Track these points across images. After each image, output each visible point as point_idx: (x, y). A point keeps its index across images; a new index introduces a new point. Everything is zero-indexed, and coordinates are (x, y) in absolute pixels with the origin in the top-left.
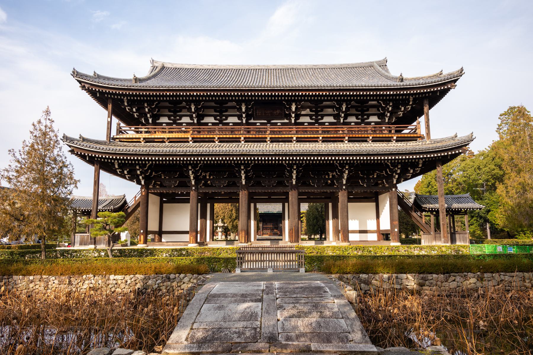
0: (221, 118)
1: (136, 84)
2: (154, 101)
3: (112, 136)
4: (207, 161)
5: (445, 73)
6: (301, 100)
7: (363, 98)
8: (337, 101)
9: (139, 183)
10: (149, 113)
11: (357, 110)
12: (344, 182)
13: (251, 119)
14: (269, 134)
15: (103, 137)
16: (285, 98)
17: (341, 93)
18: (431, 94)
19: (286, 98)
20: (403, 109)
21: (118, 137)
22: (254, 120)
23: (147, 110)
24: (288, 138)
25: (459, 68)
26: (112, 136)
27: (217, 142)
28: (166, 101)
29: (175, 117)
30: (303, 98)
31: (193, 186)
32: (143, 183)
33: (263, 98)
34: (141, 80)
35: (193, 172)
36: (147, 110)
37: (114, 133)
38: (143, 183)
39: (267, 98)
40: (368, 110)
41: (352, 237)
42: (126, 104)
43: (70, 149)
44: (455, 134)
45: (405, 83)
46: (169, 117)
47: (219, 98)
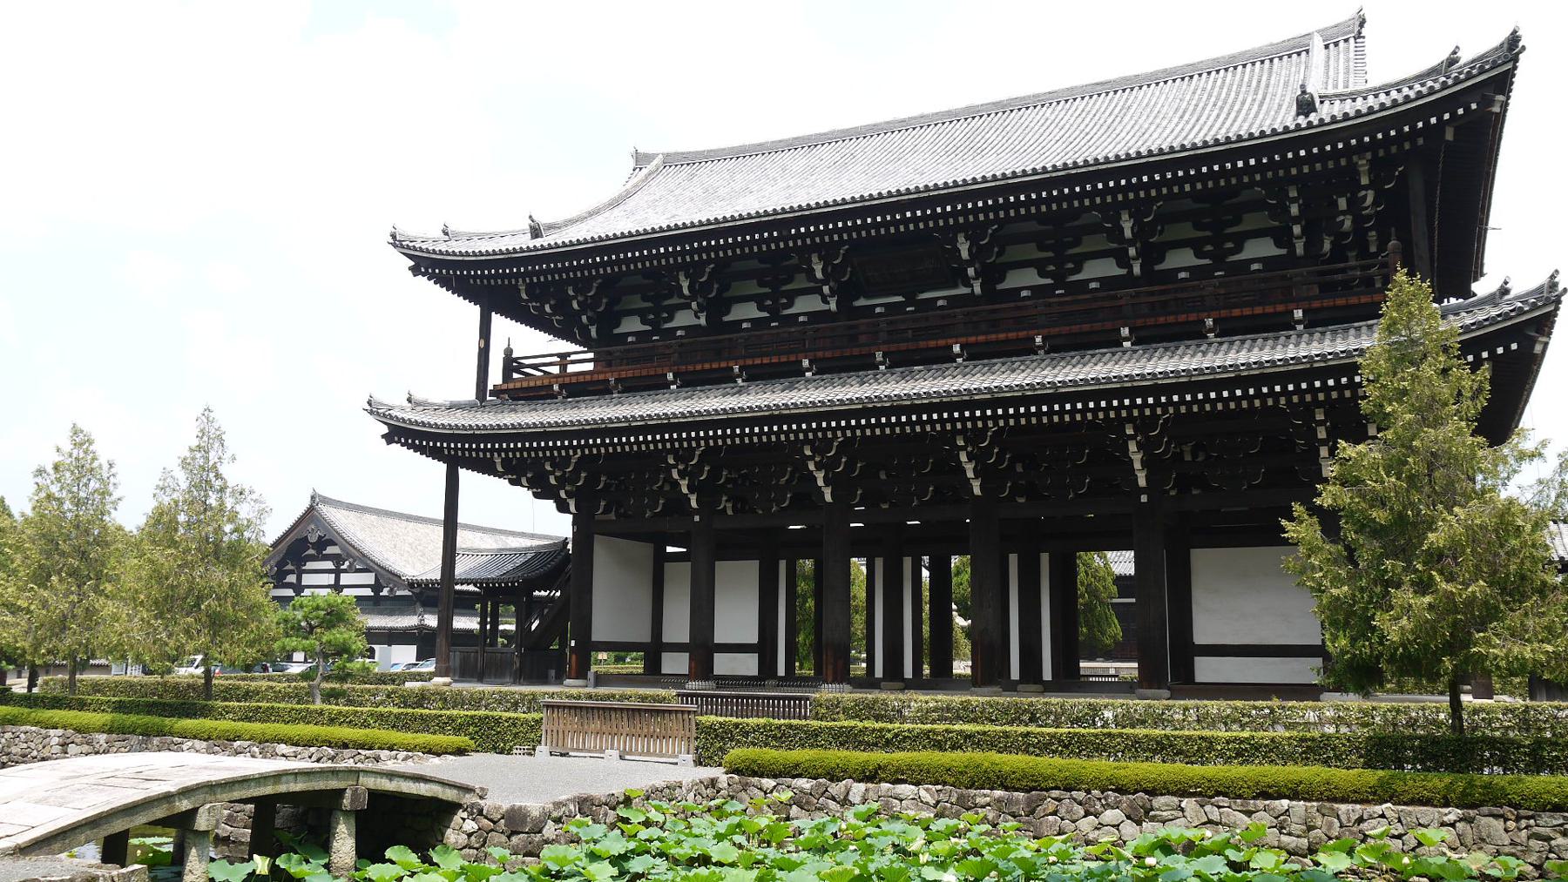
0: (775, 301)
1: (538, 242)
2: (591, 278)
3: (490, 387)
4: (786, 434)
5: (1466, 56)
6: (988, 223)
7: (1300, 170)
8: (1103, 207)
9: (562, 507)
10: (583, 310)
11: (1197, 226)
12: (1142, 482)
13: (857, 298)
14: (884, 343)
15: (470, 394)
16: (936, 223)
17: (1134, 180)
18: (1421, 141)
19: (941, 223)
20: (1342, 203)
21: (511, 386)
22: (868, 297)
23: (575, 306)
24: (938, 348)
25: (1501, 36)
26: (490, 387)
27: (739, 381)
28: (752, 255)
29: (657, 314)
30: (1087, 202)
31: (696, 512)
32: (572, 508)
33: (902, 228)
34: (551, 227)
35: (682, 474)
36: (575, 306)
37: (495, 377)
38: (572, 508)
39: (921, 226)
40: (1238, 221)
41: (1207, 670)
42: (524, 296)
43: (385, 430)
44: (1501, 283)
45: (1325, 111)
46: (642, 314)
47: (769, 247)
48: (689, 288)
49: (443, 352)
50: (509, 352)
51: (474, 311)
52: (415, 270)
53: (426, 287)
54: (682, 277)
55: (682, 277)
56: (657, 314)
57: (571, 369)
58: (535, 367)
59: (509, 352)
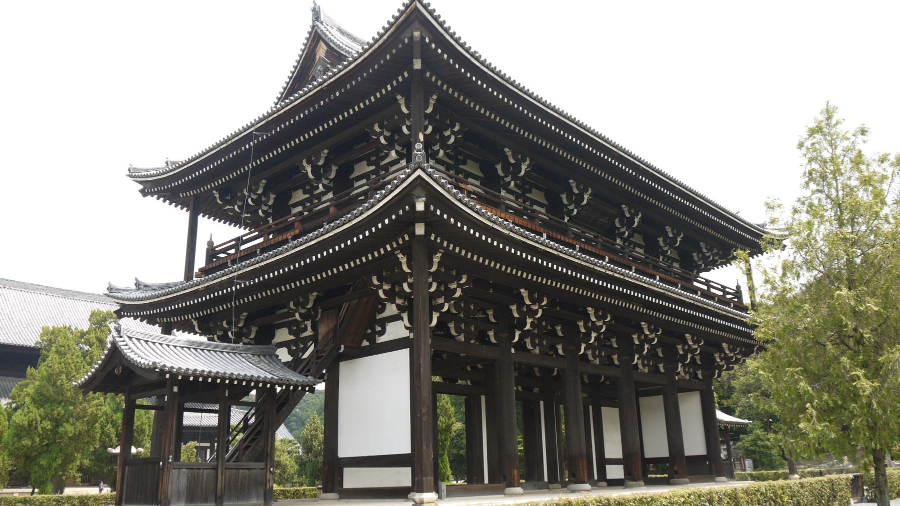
26: (196, 270)
29: (311, 202)
37: (200, 262)
42: (219, 202)
48: (312, 172)
49: (162, 247)
50: (210, 243)
51: (182, 216)
52: (144, 193)
53: (154, 203)
54: (304, 163)
55: (304, 163)
56: (311, 202)
57: (243, 247)
58: (224, 251)
59: (210, 243)
